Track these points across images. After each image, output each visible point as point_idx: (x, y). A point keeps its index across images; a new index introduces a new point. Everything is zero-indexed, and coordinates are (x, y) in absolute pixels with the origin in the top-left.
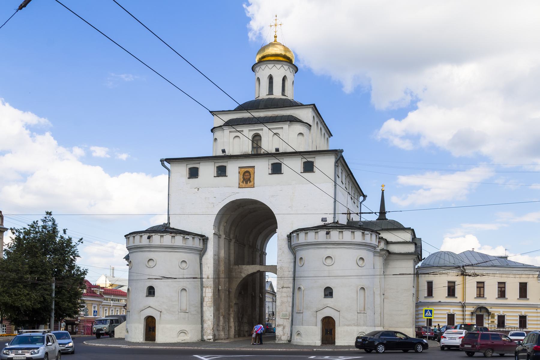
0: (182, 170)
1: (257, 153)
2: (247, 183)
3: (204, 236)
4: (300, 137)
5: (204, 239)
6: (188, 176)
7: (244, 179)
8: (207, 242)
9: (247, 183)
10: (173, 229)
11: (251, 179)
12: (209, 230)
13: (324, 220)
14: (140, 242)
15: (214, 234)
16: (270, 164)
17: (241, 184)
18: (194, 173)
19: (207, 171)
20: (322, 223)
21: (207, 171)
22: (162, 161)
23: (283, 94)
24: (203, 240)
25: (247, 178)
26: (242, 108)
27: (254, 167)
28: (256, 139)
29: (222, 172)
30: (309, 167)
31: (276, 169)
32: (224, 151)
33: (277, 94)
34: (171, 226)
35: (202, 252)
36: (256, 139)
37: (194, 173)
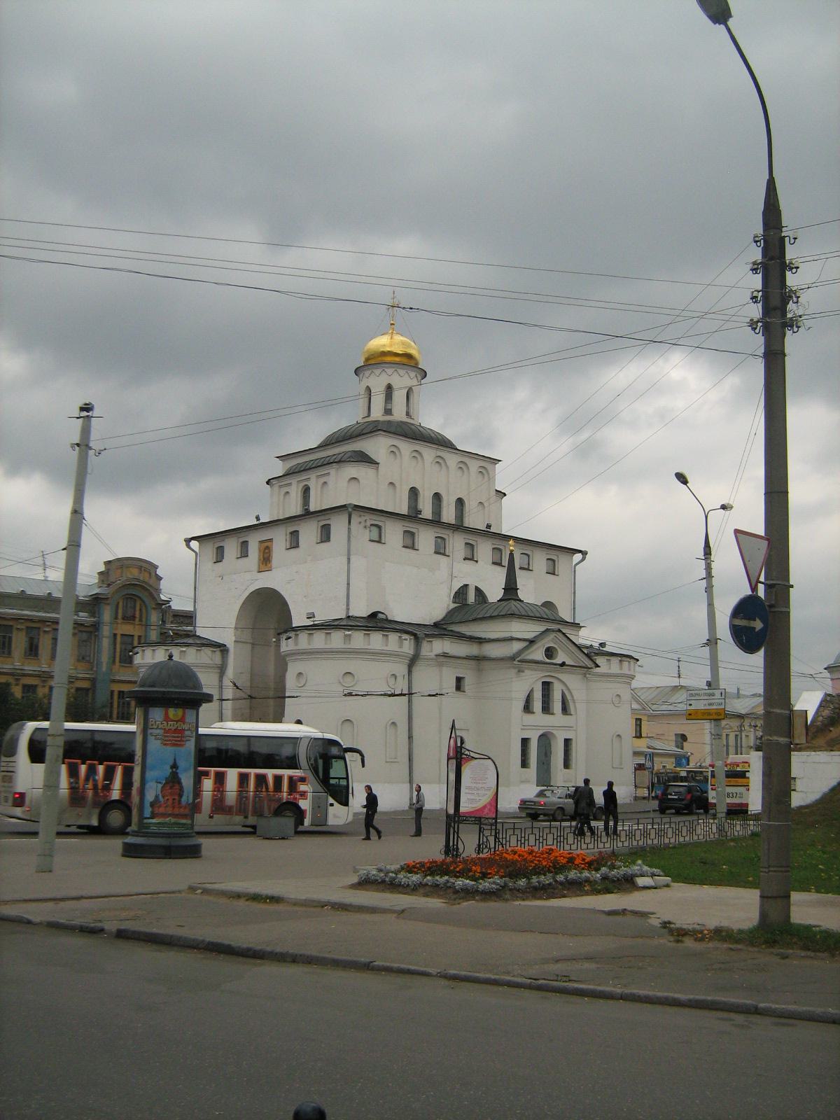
0: (210, 550)
1: (307, 514)
3: (225, 646)
4: (353, 483)
5: (222, 648)
7: (264, 559)
8: (227, 654)
9: (266, 565)
14: (143, 659)
15: (235, 641)
16: (288, 533)
18: (220, 556)
19: (231, 547)
20: (309, 622)
21: (231, 547)
22: (188, 541)
24: (221, 651)
26: (324, 445)
27: (271, 540)
32: (258, 518)
34: (198, 634)
37: (220, 556)
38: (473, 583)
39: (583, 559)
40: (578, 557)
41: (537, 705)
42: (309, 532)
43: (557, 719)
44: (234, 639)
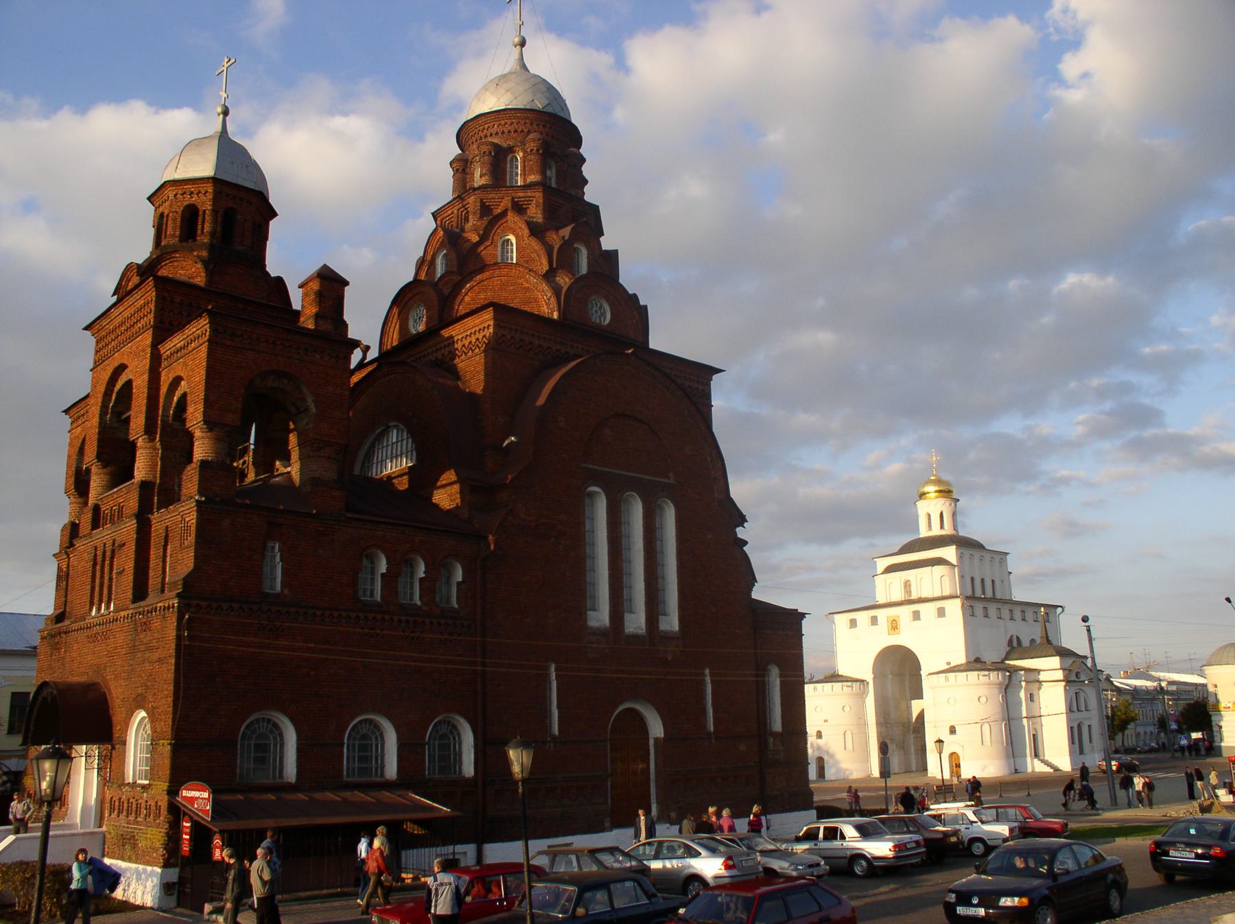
12: (869, 677)
13: (949, 663)
23: (942, 527)
25: (894, 626)
29: (874, 621)
30: (941, 613)
31: (916, 616)
33: (936, 531)
35: (862, 695)
36: (907, 585)
38: (1015, 634)
40: (1059, 610)
41: (1075, 708)
42: (927, 610)
43: (1085, 714)
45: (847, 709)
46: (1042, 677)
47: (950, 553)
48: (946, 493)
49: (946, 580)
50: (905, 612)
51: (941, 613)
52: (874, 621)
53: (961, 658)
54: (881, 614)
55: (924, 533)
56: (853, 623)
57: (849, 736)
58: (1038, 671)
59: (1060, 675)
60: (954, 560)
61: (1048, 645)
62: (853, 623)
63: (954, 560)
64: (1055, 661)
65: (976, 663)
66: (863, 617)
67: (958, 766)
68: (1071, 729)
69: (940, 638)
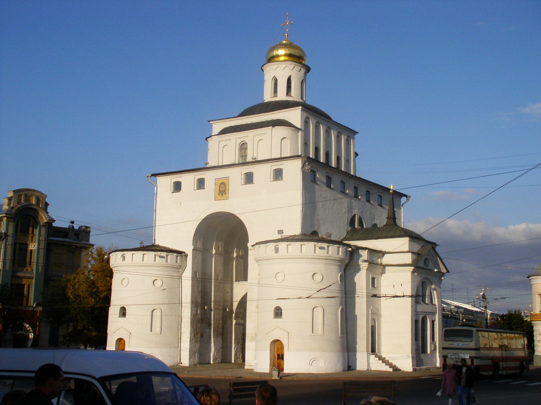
2: (222, 195)
6: (172, 191)
7: (220, 191)
9: (222, 195)
10: (158, 246)
11: (227, 191)
12: (188, 248)
17: (218, 196)
25: (222, 190)
28: (243, 147)
29: (201, 184)
30: (278, 174)
31: (249, 178)
33: (282, 96)
34: (157, 243)
36: (243, 147)
39: (408, 200)
40: (403, 199)
42: (263, 172)
44: (192, 247)
45: (158, 283)
46: (386, 260)
47: (295, 116)
48: (297, 58)
49: (287, 144)
50: (236, 176)
51: (278, 174)
52: (201, 184)
53: (297, 230)
54: (210, 177)
55: (268, 97)
56: (178, 187)
57: (157, 313)
58: (383, 253)
59: (408, 258)
60: (298, 123)
61: (392, 229)
62: (178, 187)
63: (298, 123)
64: (403, 243)
65: (310, 235)
66: (188, 180)
67: (281, 357)
68: (415, 323)
69: (273, 205)
